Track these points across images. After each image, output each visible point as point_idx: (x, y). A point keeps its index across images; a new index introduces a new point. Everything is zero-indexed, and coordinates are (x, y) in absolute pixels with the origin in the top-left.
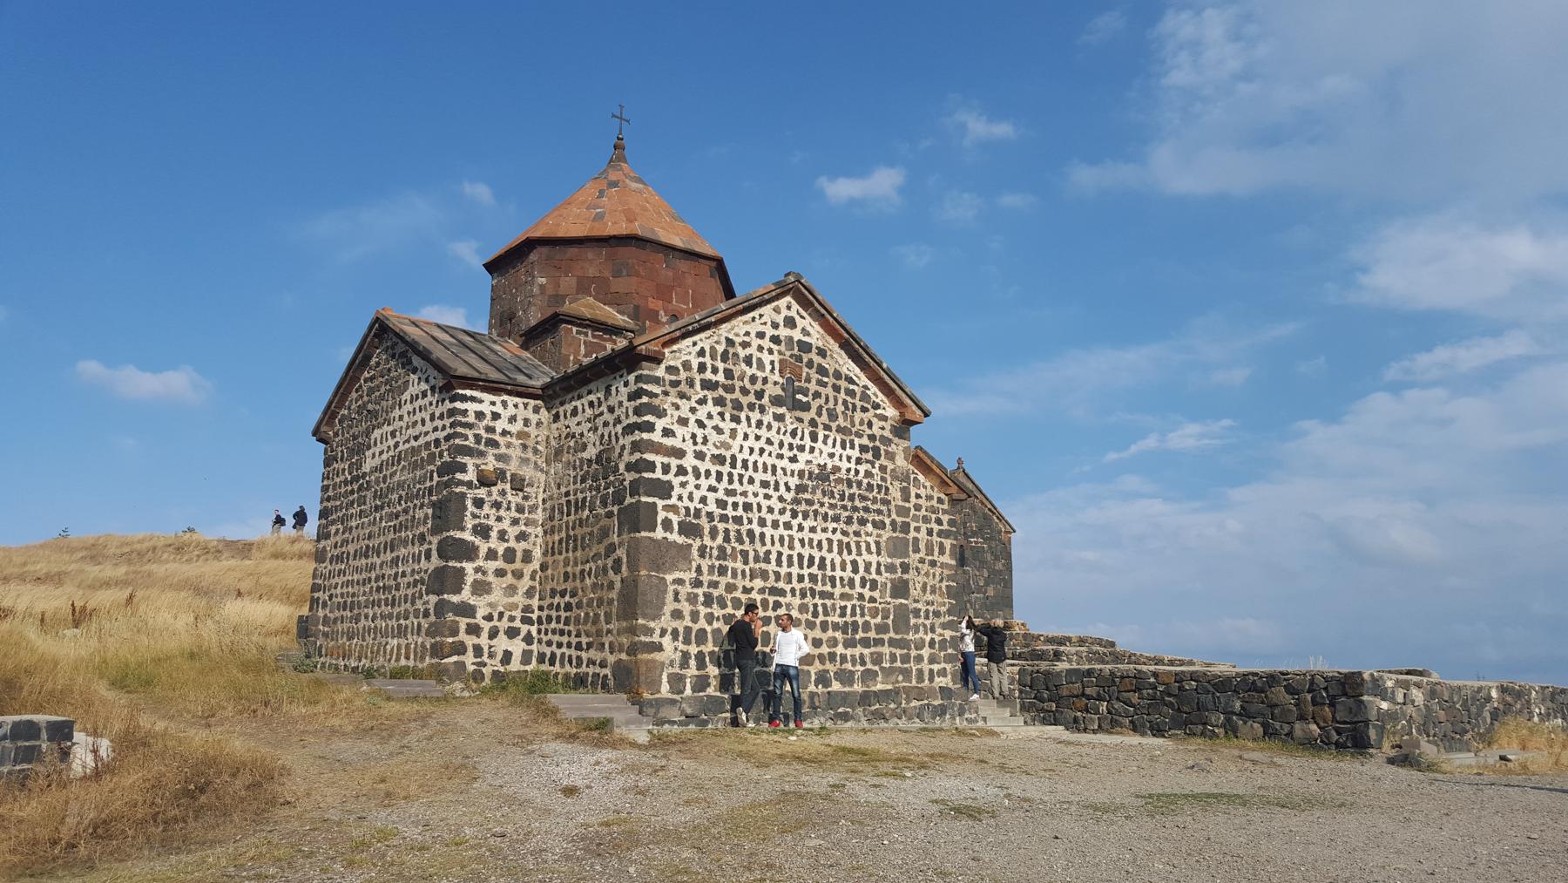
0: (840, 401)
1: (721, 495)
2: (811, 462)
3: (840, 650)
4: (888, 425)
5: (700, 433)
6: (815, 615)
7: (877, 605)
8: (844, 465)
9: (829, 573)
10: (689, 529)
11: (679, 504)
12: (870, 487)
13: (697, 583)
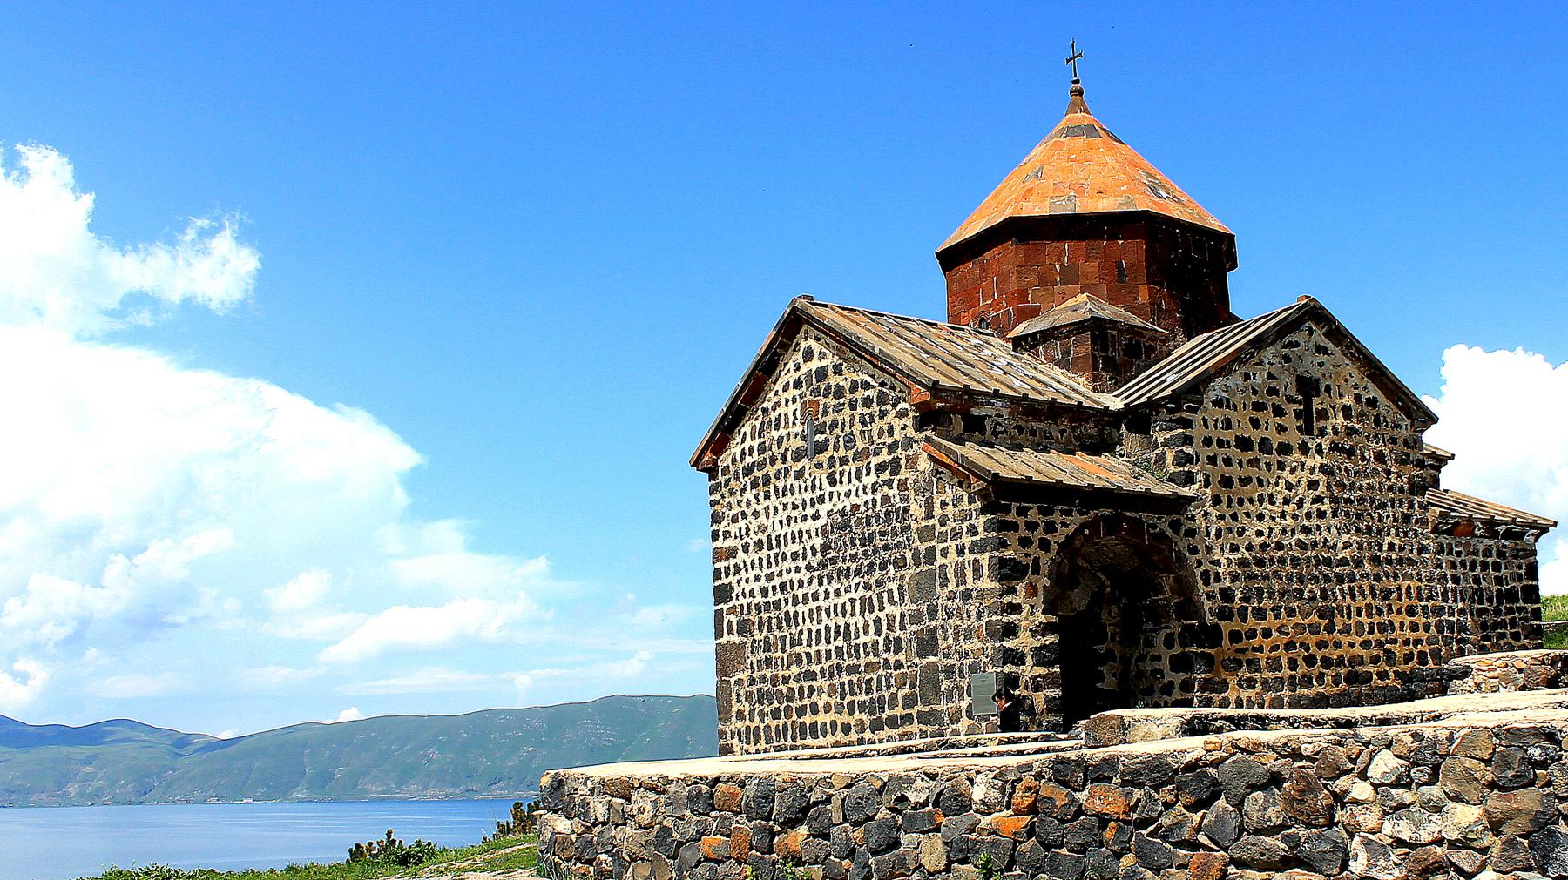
0: (857, 420)
1: (763, 583)
2: (832, 511)
3: (868, 735)
4: (909, 421)
5: (742, 524)
7: (904, 671)
9: (854, 642)
10: (744, 628)
11: (737, 603)
12: (887, 514)
13: (752, 681)
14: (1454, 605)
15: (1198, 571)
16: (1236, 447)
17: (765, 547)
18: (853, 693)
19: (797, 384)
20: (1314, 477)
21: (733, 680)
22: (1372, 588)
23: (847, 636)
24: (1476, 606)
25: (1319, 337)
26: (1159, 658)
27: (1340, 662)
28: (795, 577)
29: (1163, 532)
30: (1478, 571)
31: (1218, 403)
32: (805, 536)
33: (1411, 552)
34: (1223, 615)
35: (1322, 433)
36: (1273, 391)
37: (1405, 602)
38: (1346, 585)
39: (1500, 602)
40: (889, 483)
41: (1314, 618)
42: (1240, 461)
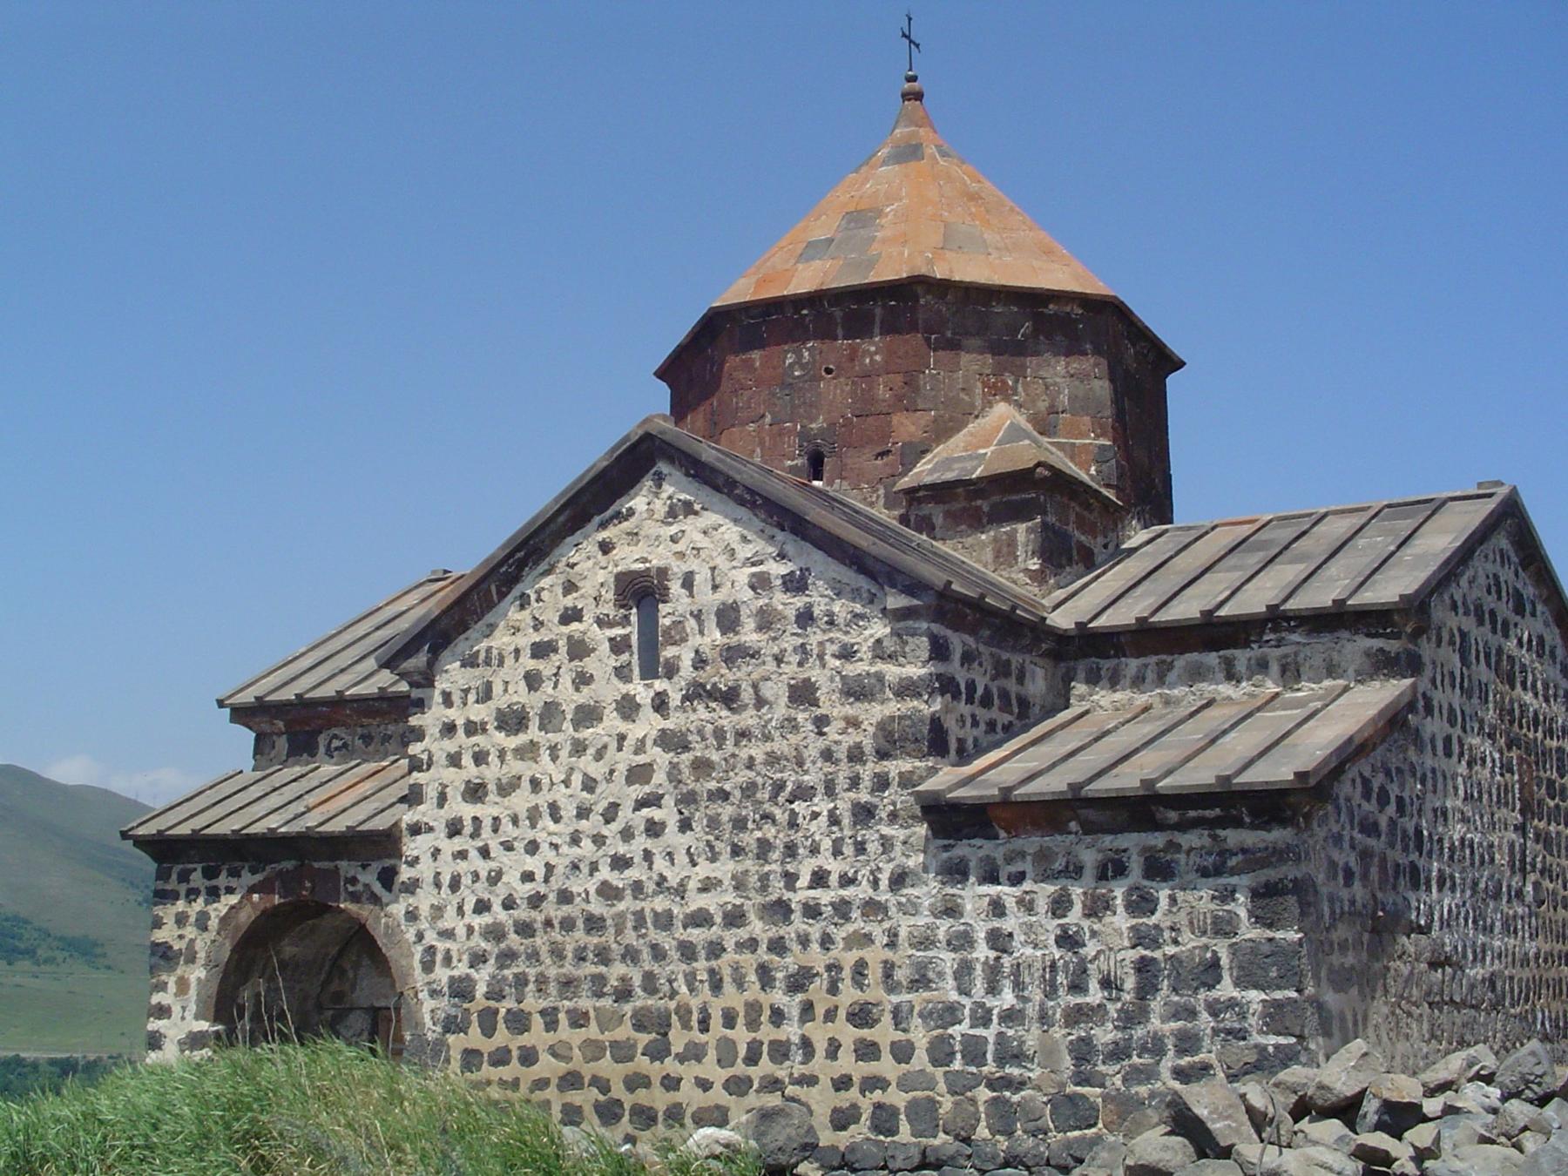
14: (990, 1002)
15: (420, 948)
16: (499, 728)
20: (641, 759)
24: (1068, 1000)
25: (675, 488)
29: (367, 886)
33: (875, 883)
34: (453, 1025)
35: (671, 671)
37: (849, 994)
38: (701, 964)
39: (1146, 989)
41: (625, 1032)
42: (502, 754)
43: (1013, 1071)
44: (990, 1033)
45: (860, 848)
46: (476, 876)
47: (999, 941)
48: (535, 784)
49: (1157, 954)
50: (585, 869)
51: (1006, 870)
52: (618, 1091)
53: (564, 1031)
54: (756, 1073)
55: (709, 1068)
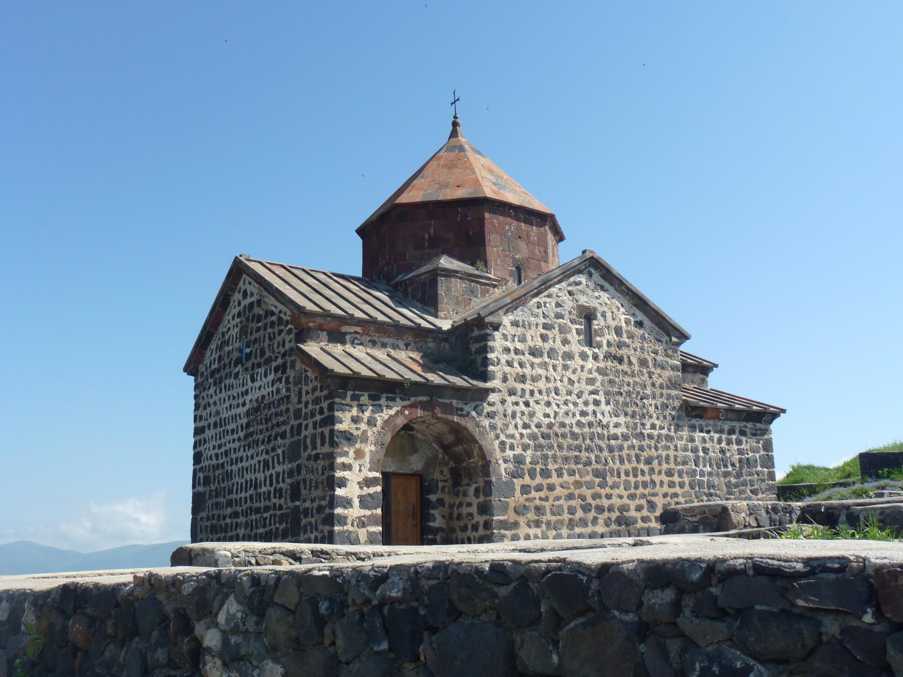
0: (267, 335)
1: (216, 451)
4: (292, 336)
6: (251, 531)
8: (264, 392)
9: (259, 491)
11: (204, 465)
13: (208, 519)
14: (705, 469)
15: (497, 442)
17: (219, 426)
18: (257, 528)
19: (239, 315)
20: (591, 376)
21: (199, 518)
22: (638, 457)
23: (255, 488)
24: (723, 469)
26: (469, 505)
27: (610, 509)
28: (233, 446)
30: (723, 445)
31: (515, 324)
32: (238, 418)
34: (516, 475)
35: (599, 346)
36: (559, 316)
37: (665, 466)
38: (616, 454)
39: (741, 468)
40: (280, 380)
41: (588, 478)
42: (532, 365)
43: (712, 491)
44: (705, 479)
45: (665, 417)
46: (523, 413)
47: (705, 450)
48: (547, 378)
49: (743, 457)
50: (571, 415)
51: (705, 429)
52: (589, 500)
53: (566, 477)
54: (638, 492)
55: (621, 491)
